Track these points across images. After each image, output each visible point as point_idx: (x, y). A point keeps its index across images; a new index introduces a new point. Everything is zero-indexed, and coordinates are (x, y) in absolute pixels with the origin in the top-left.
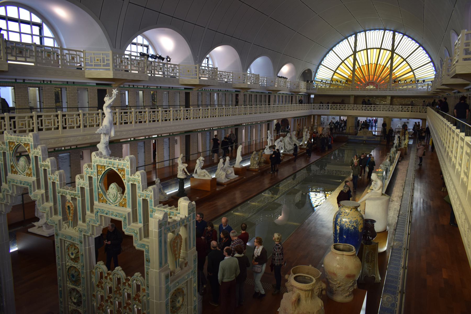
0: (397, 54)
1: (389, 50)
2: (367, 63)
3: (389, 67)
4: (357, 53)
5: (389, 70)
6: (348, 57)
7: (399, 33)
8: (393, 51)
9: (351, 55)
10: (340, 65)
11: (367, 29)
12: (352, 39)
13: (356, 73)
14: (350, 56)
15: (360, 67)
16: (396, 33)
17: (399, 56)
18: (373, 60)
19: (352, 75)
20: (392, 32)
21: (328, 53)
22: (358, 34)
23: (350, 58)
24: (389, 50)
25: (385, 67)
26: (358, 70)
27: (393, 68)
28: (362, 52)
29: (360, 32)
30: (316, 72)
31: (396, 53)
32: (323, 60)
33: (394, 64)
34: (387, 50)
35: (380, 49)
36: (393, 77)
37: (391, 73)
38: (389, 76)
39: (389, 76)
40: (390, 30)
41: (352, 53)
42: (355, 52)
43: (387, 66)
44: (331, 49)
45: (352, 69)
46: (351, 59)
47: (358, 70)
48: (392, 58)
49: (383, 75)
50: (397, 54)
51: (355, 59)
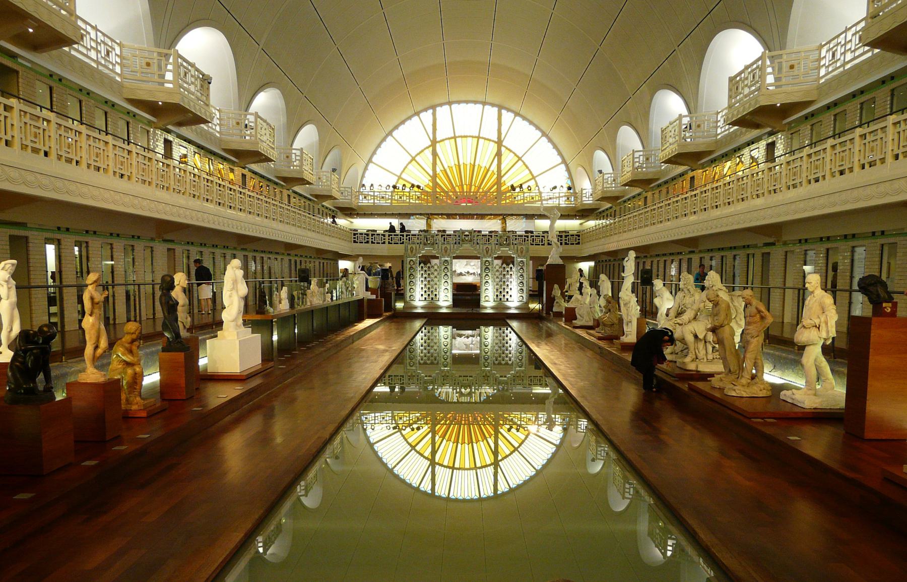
0: (507, 148)
1: (493, 141)
2: (457, 163)
3: (496, 170)
4: (438, 145)
5: (496, 176)
6: (422, 151)
7: (509, 110)
8: (499, 143)
9: (428, 148)
10: (407, 165)
11: (452, 99)
12: (427, 116)
13: (438, 180)
14: (425, 149)
15: (445, 170)
16: (504, 112)
17: (511, 151)
18: (466, 159)
19: (431, 184)
20: (495, 110)
21: (384, 140)
22: (438, 109)
23: (426, 151)
24: (493, 141)
25: (488, 170)
26: (441, 174)
27: (503, 173)
28: (447, 142)
29: (441, 105)
30: (363, 176)
31: (505, 147)
32: (374, 153)
33: (503, 166)
34: (490, 140)
35: (479, 138)
36: (502, 188)
37: (499, 183)
38: (496, 187)
39: (496, 187)
40: (493, 105)
41: (430, 143)
42: (434, 143)
43: (491, 169)
44: (390, 133)
45: (431, 173)
46: (428, 153)
47: (441, 174)
48: (499, 154)
49: (486, 186)
50: (507, 148)
51: (435, 154)
